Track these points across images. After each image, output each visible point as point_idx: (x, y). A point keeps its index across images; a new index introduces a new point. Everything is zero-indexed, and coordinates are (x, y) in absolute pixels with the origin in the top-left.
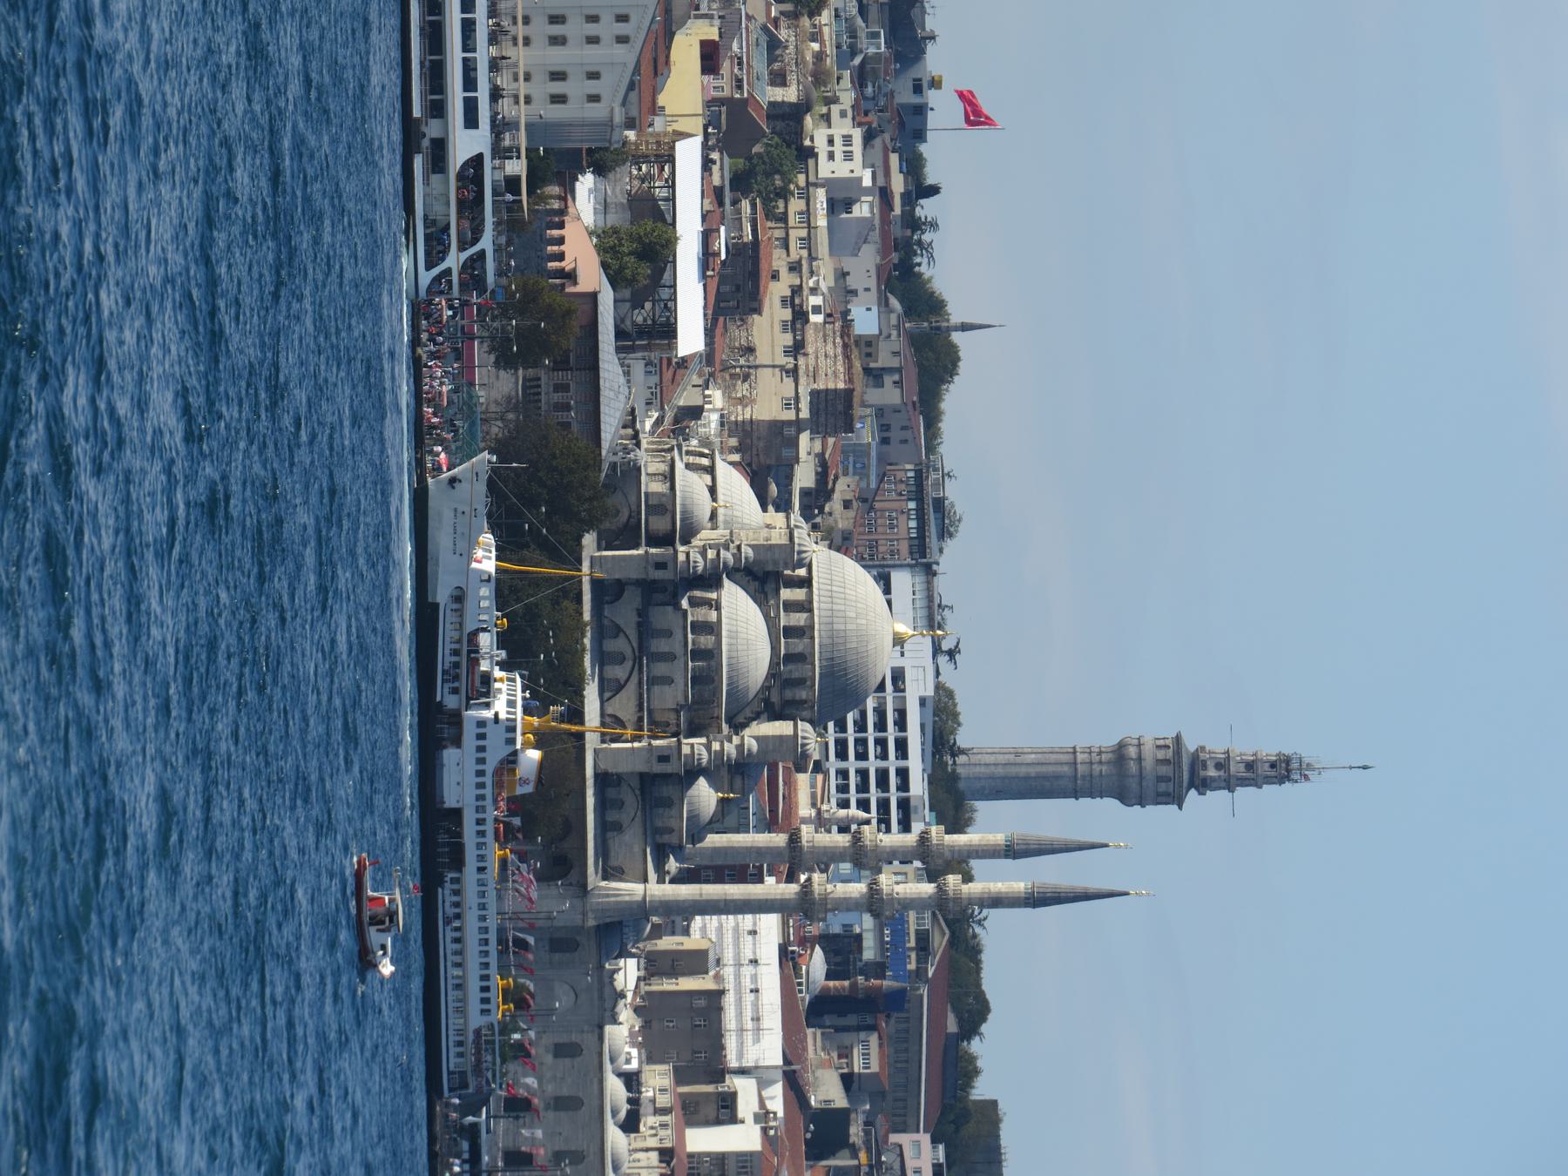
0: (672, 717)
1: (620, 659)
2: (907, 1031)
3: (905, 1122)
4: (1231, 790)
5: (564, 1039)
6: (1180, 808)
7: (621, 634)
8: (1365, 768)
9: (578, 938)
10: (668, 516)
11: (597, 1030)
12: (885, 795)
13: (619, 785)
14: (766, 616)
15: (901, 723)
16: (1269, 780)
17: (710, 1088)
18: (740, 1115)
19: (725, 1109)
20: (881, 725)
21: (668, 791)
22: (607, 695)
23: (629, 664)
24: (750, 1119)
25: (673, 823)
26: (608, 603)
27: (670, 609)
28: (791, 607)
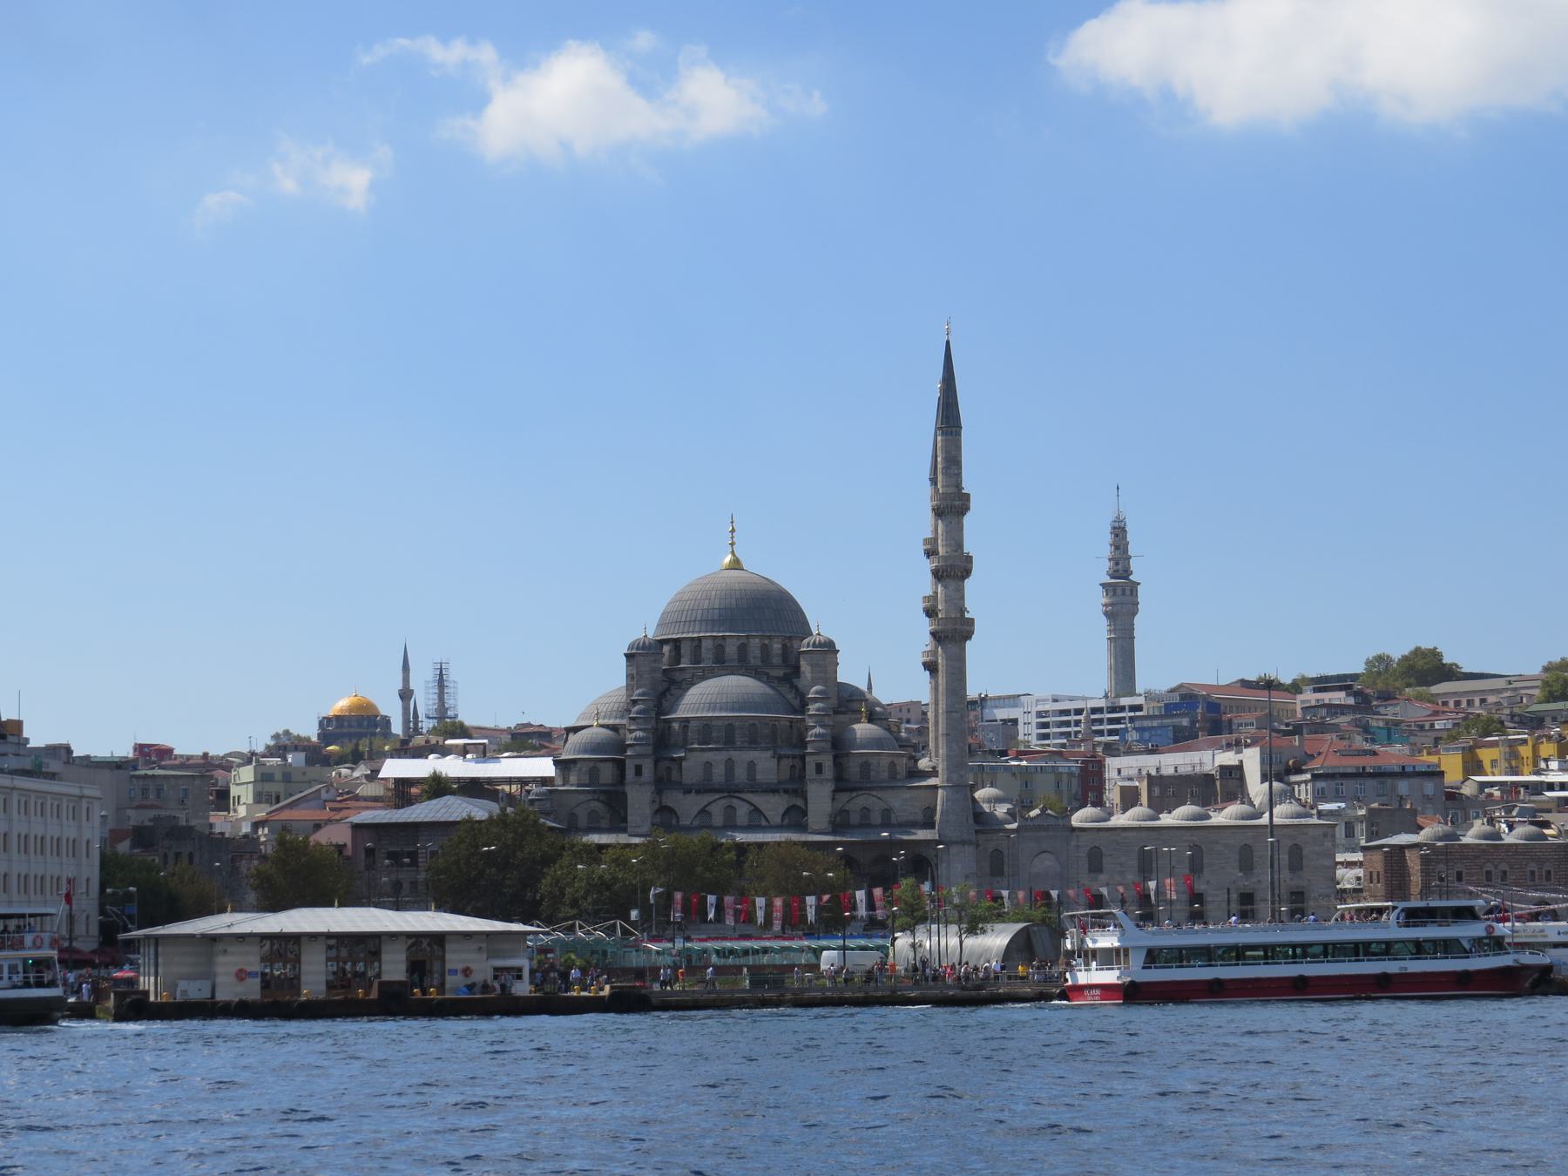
0: (786, 763)
1: (730, 809)
2: (1238, 707)
3: (1292, 711)
4: (1130, 557)
5: (1084, 864)
6: (1139, 584)
7: (707, 809)
8: (1118, 488)
9: (991, 850)
10: (601, 766)
12: (1105, 720)
13: (846, 811)
14: (704, 678)
15: (1066, 712)
16: (1125, 537)
17: (1218, 783)
18: (1237, 763)
19: (1234, 774)
20: (1067, 724)
21: (853, 769)
22: (764, 823)
23: (735, 801)
24: (1240, 757)
25: (885, 762)
26: (678, 822)
27: (684, 764)
28: (697, 659)
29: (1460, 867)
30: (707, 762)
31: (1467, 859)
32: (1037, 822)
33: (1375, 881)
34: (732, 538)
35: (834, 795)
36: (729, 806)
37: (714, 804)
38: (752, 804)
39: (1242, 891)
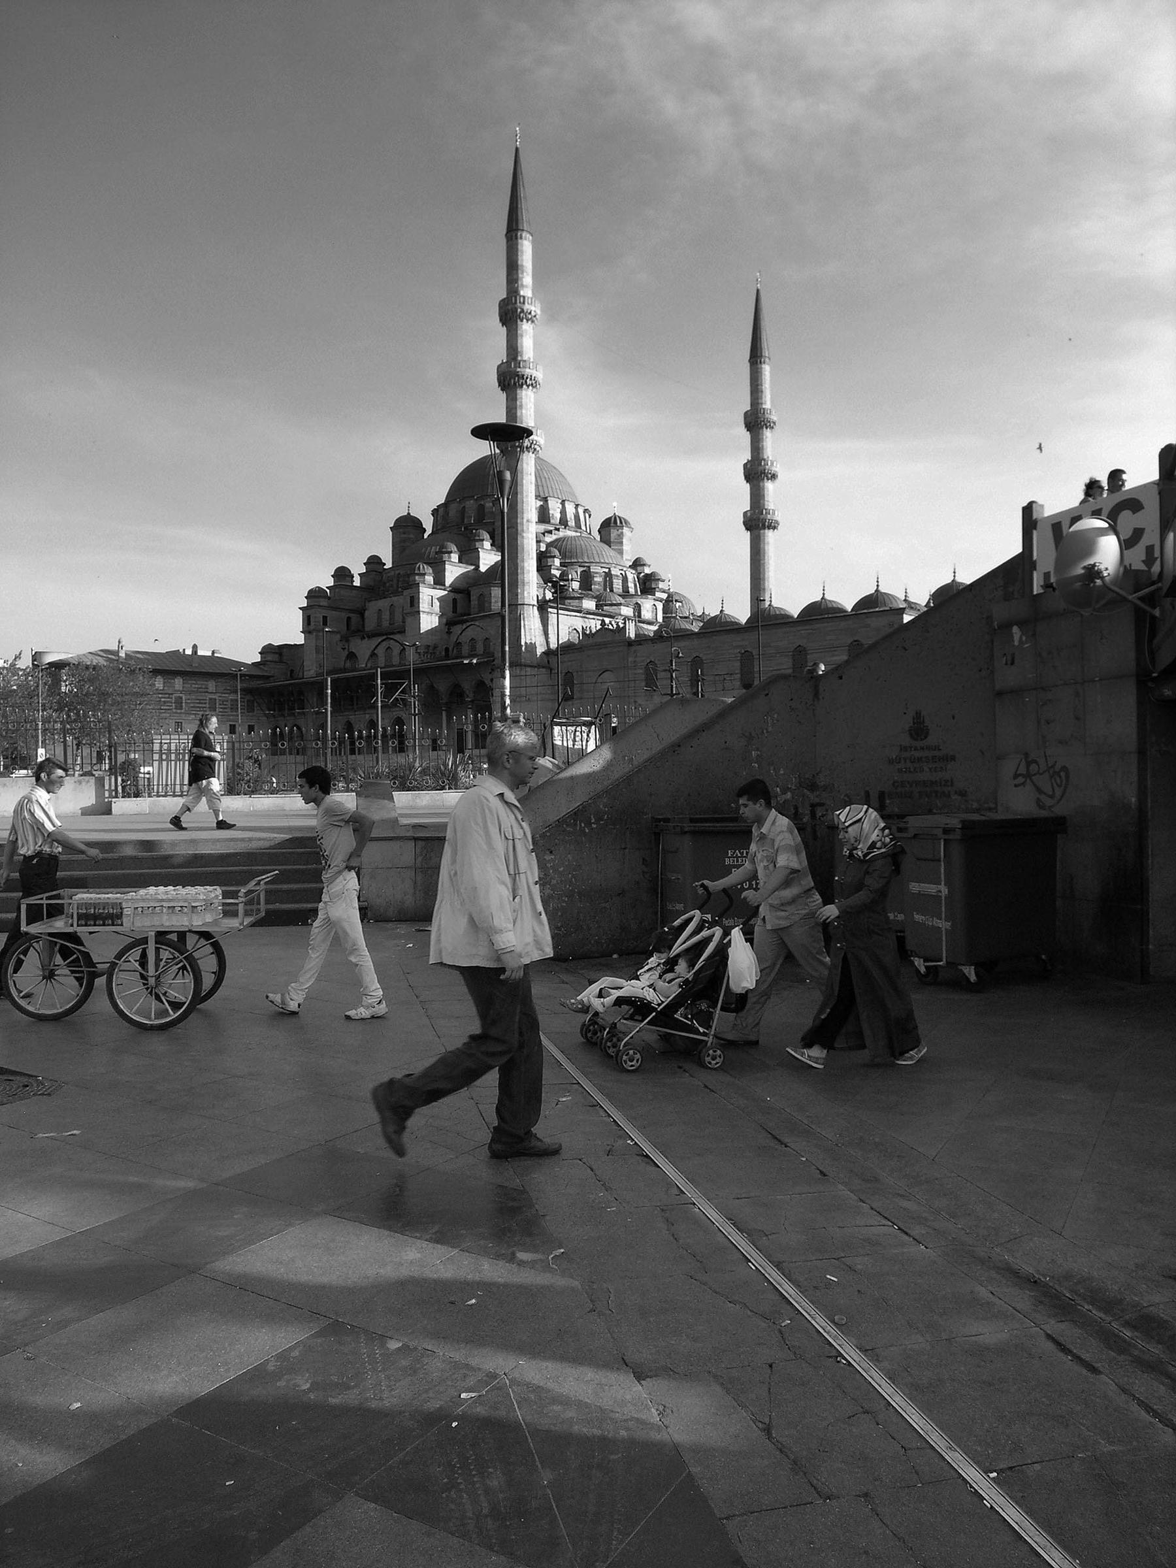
11: (633, 648)
23: (392, 641)
30: (380, 610)
32: (599, 640)
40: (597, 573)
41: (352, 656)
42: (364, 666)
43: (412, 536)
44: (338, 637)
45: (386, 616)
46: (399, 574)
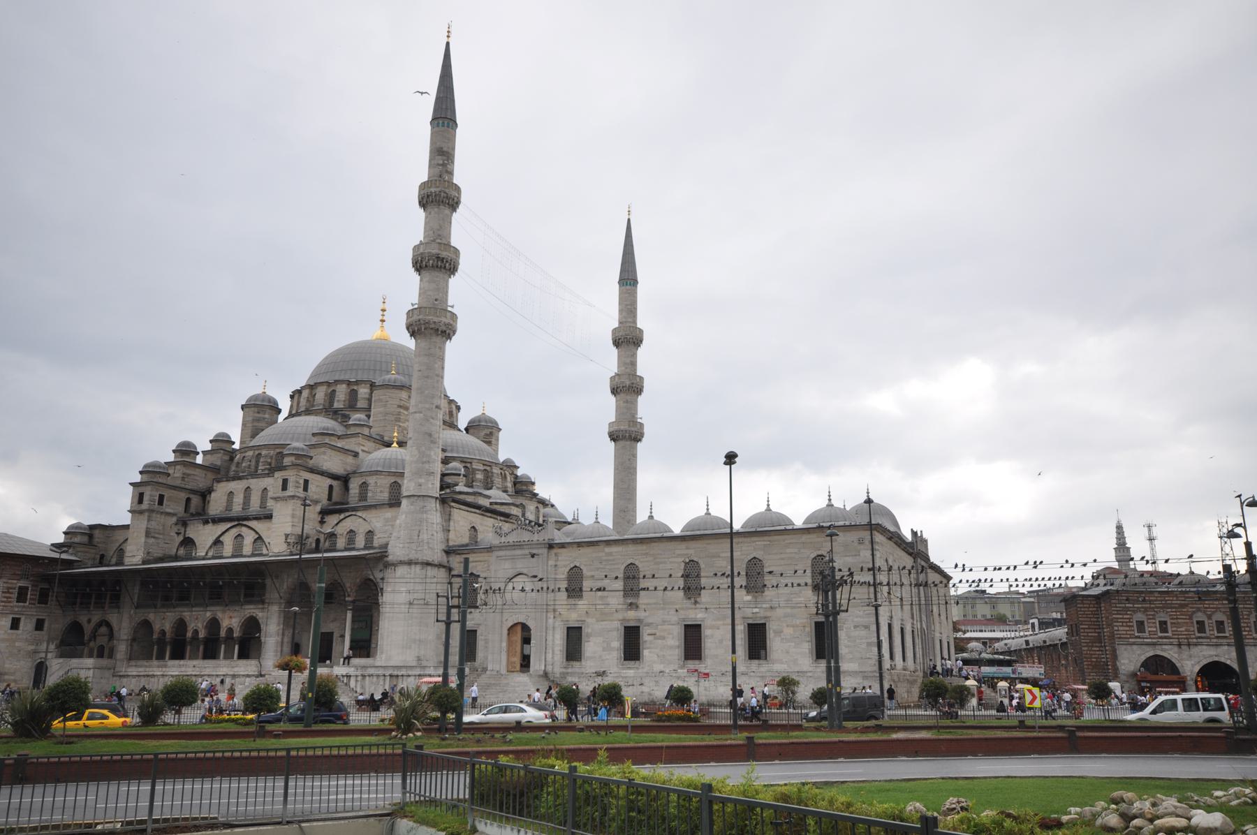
7: (221, 539)
11: (555, 551)
23: (244, 529)
29: (1162, 616)
31: (1171, 608)
33: (1075, 634)
34: (383, 315)
35: (322, 518)
36: (239, 535)
37: (227, 533)
38: (257, 533)
39: (751, 622)
40: (479, 470)
41: (188, 542)
42: (204, 554)
43: (267, 416)
44: (174, 519)
45: (238, 499)
46: (260, 454)
